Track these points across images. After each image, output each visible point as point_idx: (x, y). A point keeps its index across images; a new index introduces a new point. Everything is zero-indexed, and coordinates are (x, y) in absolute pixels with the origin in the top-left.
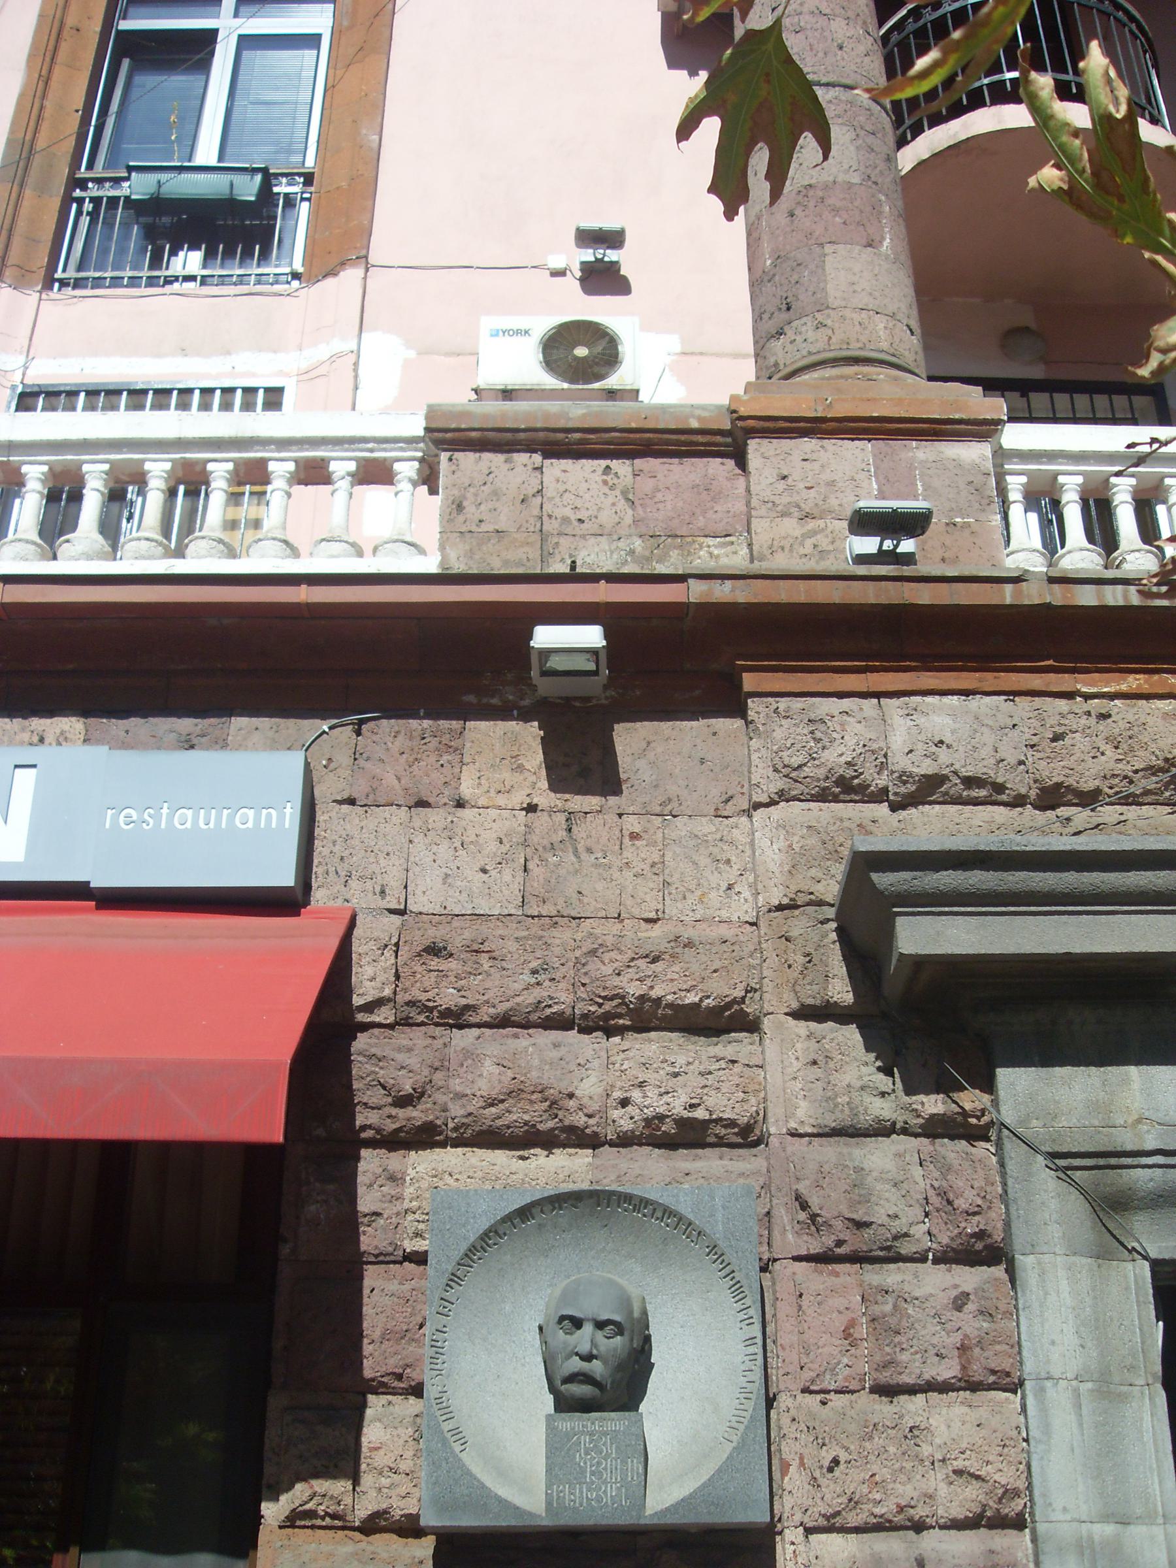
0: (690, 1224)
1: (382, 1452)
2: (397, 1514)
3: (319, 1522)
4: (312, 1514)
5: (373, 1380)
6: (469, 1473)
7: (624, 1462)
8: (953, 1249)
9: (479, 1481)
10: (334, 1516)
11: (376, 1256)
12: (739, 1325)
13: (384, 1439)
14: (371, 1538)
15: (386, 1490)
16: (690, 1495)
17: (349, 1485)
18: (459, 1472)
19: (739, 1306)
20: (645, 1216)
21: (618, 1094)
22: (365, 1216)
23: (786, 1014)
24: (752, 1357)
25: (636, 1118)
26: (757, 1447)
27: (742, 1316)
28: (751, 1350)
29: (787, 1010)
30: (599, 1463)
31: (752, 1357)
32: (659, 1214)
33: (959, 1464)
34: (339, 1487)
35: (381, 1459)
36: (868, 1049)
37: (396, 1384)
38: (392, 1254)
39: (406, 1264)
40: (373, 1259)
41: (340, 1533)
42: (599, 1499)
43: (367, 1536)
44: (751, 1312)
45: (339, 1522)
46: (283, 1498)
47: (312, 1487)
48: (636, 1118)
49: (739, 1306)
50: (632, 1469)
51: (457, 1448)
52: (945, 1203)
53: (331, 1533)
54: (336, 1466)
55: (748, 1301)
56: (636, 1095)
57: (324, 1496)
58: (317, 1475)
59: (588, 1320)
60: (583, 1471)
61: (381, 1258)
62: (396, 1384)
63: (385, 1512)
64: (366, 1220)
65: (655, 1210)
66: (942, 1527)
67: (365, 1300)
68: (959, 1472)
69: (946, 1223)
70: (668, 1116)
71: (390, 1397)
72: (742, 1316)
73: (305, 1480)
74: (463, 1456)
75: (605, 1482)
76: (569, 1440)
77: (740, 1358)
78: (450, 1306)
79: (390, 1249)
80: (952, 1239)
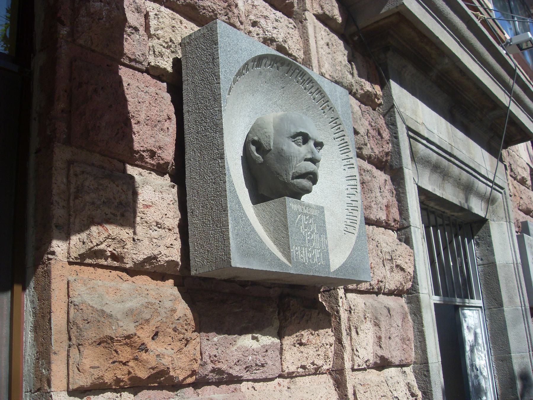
0: (328, 101)
1: (152, 209)
2: (163, 260)
3: (102, 262)
4: (101, 254)
5: (138, 152)
8: (378, 158)
10: (114, 257)
11: (131, 60)
12: (343, 167)
13: (153, 200)
14: (134, 279)
15: (154, 240)
17: (131, 231)
19: (344, 156)
20: (305, 89)
21: (252, 17)
22: (130, 27)
23: (314, 14)
24: (353, 187)
25: (261, 36)
28: (353, 182)
29: (315, 13)
31: (353, 187)
32: (313, 90)
33: (399, 262)
34: (124, 233)
35: (152, 215)
36: (346, 48)
37: (149, 160)
38: (141, 63)
39: (145, 74)
40: (127, 62)
41: (114, 273)
43: (132, 276)
45: (117, 263)
46: (75, 239)
47: (107, 230)
48: (261, 36)
49: (344, 156)
52: (377, 134)
53: (107, 272)
54: (123, 215)
56: (262, 21)
57: (114, 239)
58: (109, 222)
59: (313, 139)
61: (133, 64)
62: (149, 160)
63: (155, 258)
64: (129, 30)
65: (313, 86)
66: (384, 294)
67: (126, 91)
68: (397, 266)
69: (377, 144)
70: (275, 41)
71: (140, 170)
72: (345, 162)
73: (100, 224)
77: (345, 186)
79: (142, 59)
80: (380, 152)
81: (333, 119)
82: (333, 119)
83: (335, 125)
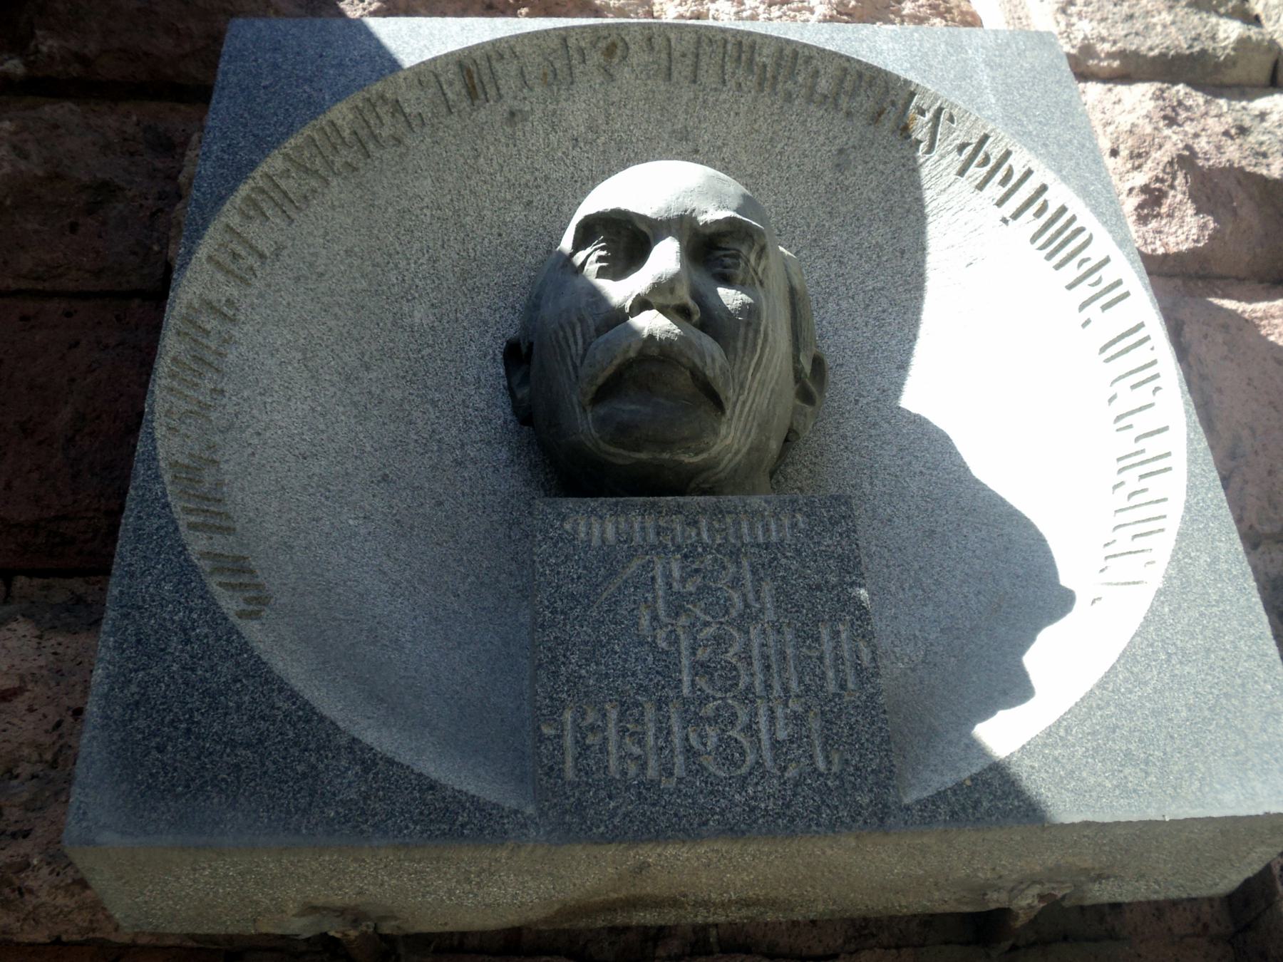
6: (260, 672)
7: (808, 636)
9: (294, 696)
16: (1049, 732)
18: (226, 669)
19: (1072, 271)
26: (1230, 590)
27: (1085, 291)
30: (718, 640)
42: (729, 752)
44: (1108, 274)
49: (1072, 271)
50: (838, 658)
51: (230, 604)
55: (1094, 254)
60: (667, 667)
72: (1085, 291)
74: (252, 630)
75: (747, 696)
76: (612, 573)
78: (252, 261)
81: (969, 150)
82: (969, 150)
83: (988, 168)
